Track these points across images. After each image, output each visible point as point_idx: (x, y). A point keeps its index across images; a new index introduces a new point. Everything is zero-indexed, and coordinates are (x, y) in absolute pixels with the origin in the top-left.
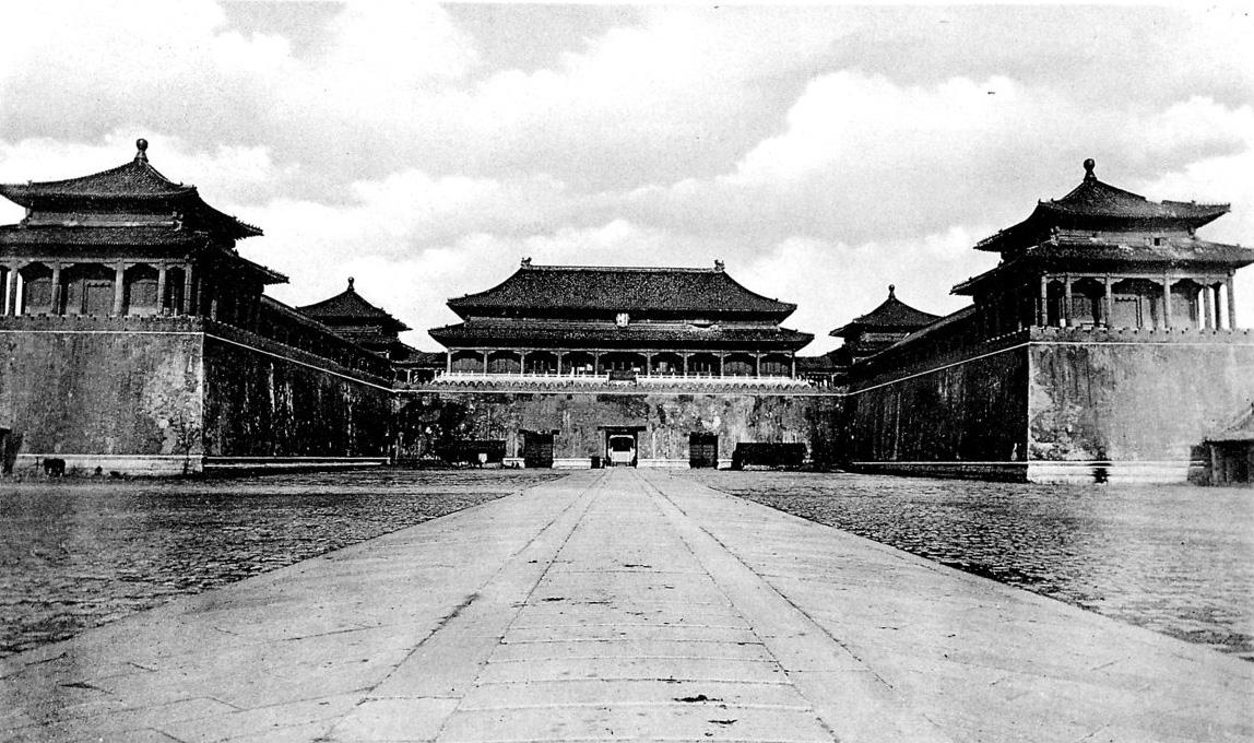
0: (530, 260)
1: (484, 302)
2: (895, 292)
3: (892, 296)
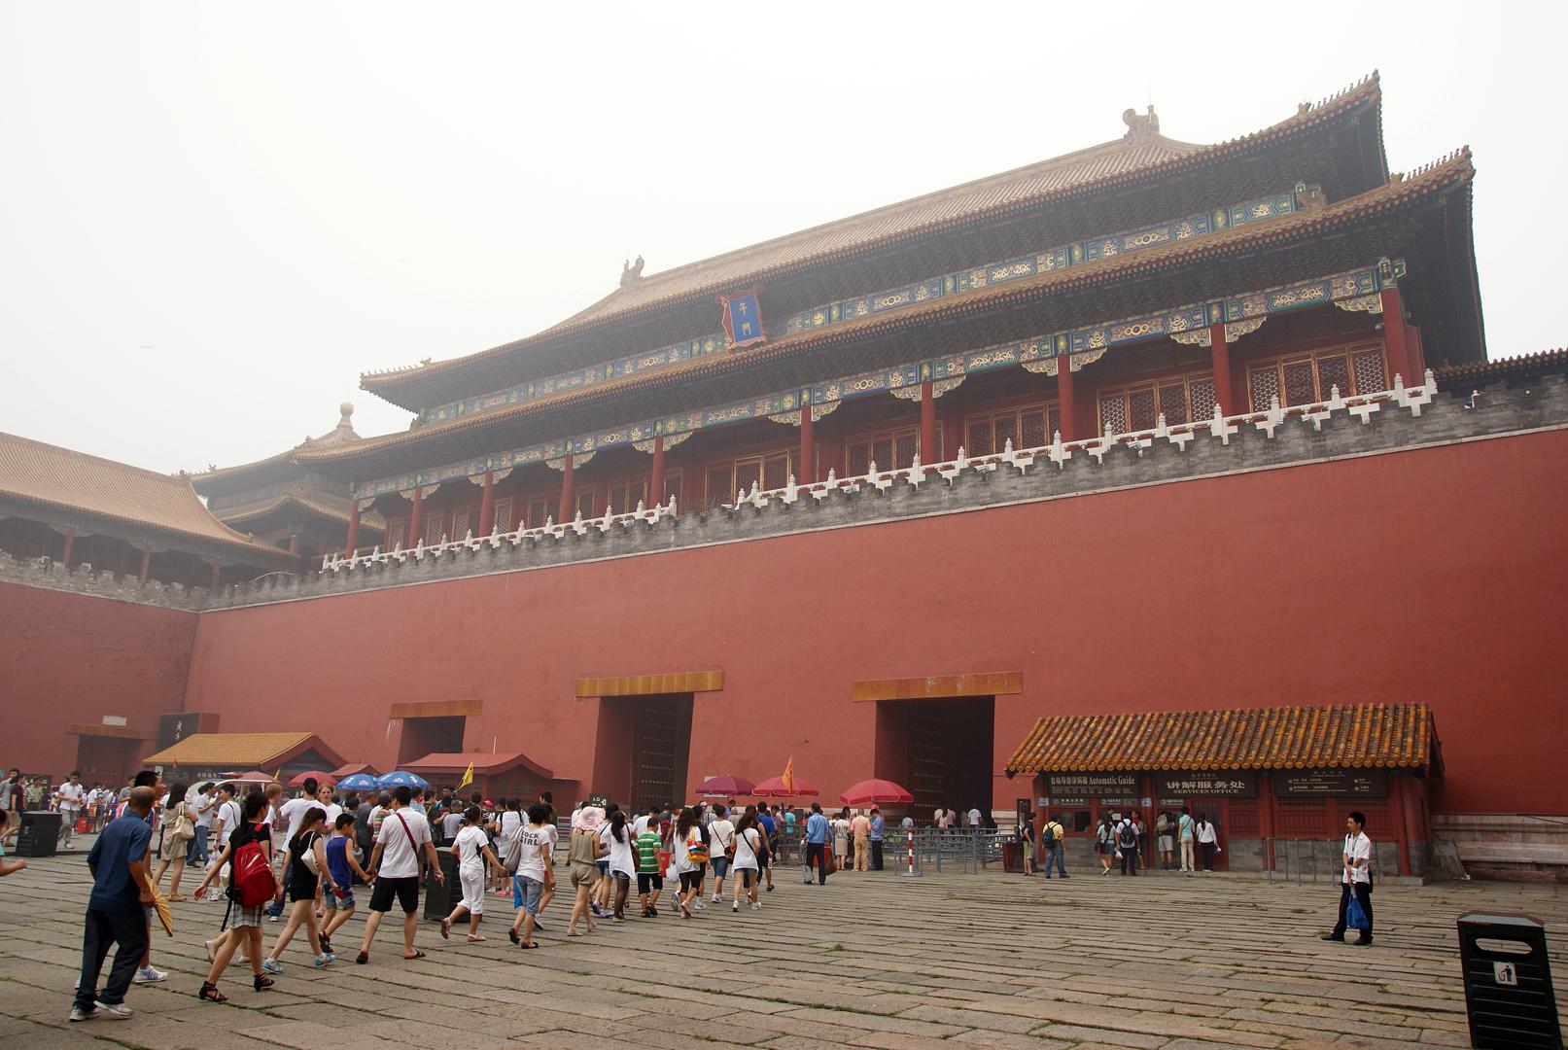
0: (640, 263)
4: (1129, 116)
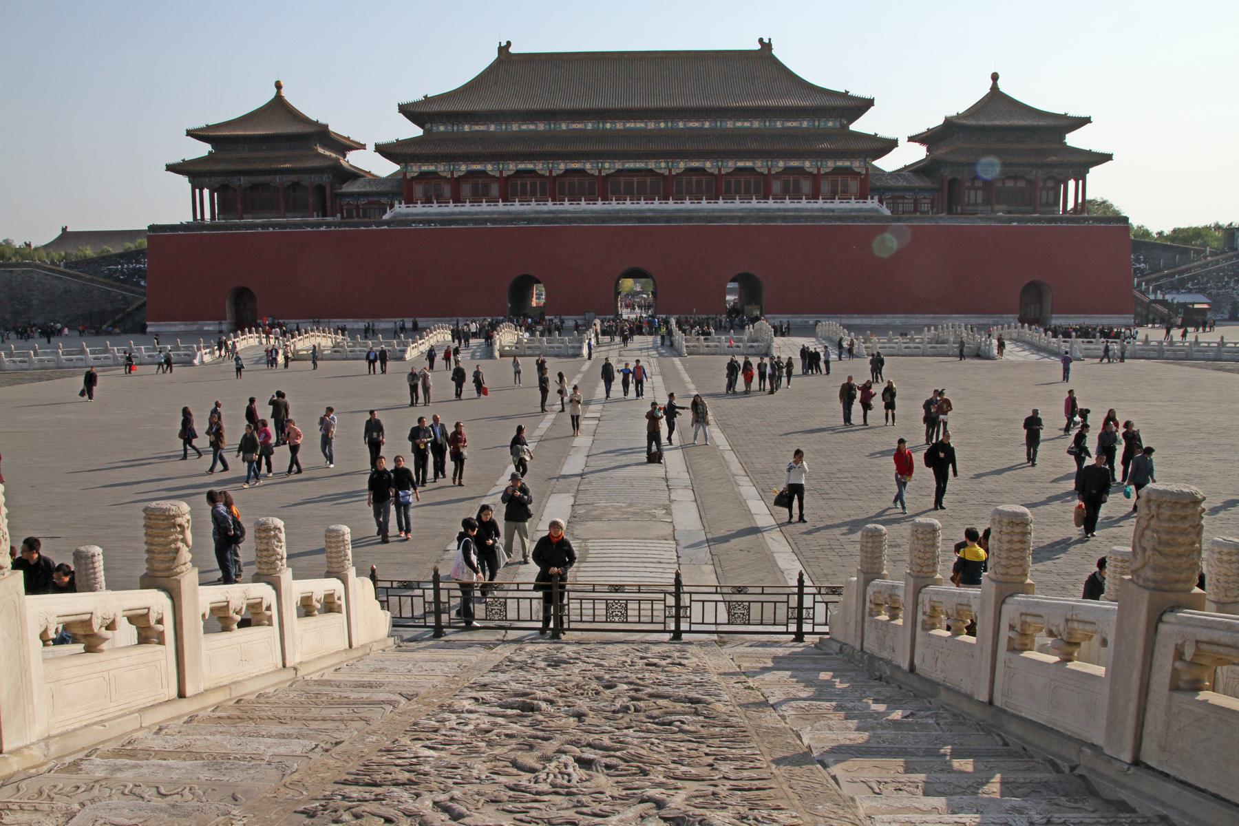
0: (509, 43)
1: (444, 107)
2: (999, 82)
3: (995, 88)
4: (761, 41)
